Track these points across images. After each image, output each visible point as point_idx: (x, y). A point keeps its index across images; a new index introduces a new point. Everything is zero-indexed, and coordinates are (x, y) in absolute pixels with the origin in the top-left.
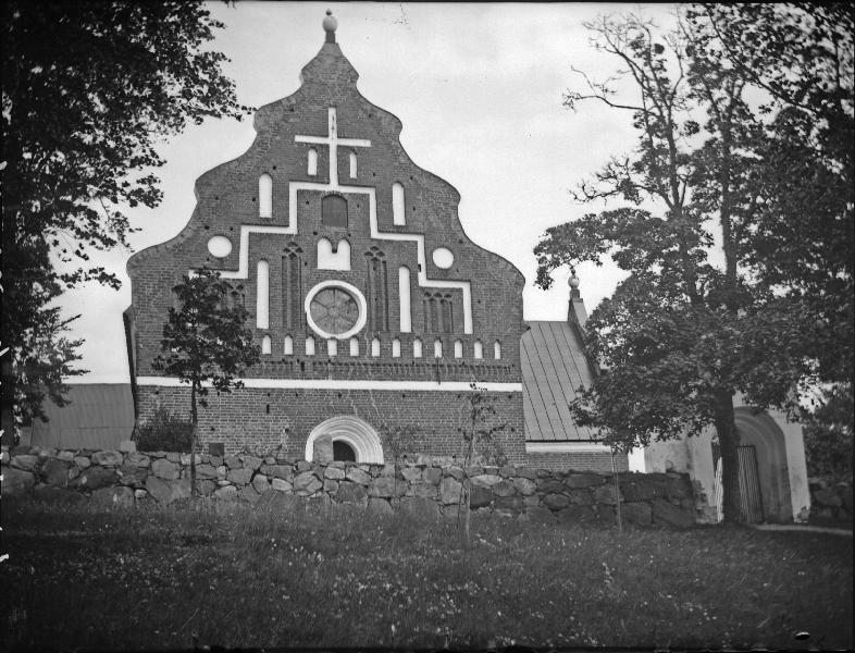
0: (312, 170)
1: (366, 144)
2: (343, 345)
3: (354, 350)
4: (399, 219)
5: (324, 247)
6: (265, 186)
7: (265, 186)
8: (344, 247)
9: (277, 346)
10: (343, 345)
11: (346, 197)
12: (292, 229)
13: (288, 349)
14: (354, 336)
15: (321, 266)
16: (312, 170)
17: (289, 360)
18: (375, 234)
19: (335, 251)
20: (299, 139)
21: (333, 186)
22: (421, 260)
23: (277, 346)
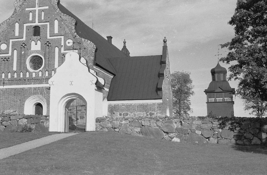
0: (31, 19)
1: (47, 7)
2: (37, 74)
3: (40, 75)
4: (56, 31)
5: (33, 43)
6: (17, 25)
7: (17, 25)
8: (39, 43)
9: (19, 75)
10: (37, 74)
11: (40, 26)
12: (24, 39)
13: (21, 76)
14: (40, 71)
15: (32, 49)
16: (31, 19)
17: (21, 79)
18: (48, 37)
19: (36, 44)
20: (27, 9)
21: (37, 23)
22: (63, 44)
23: (19, 75)
